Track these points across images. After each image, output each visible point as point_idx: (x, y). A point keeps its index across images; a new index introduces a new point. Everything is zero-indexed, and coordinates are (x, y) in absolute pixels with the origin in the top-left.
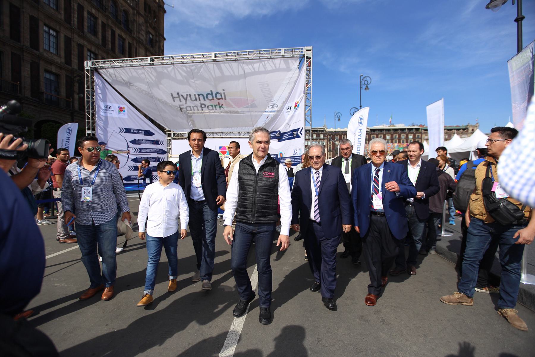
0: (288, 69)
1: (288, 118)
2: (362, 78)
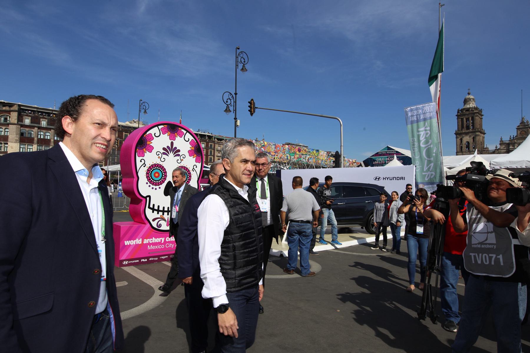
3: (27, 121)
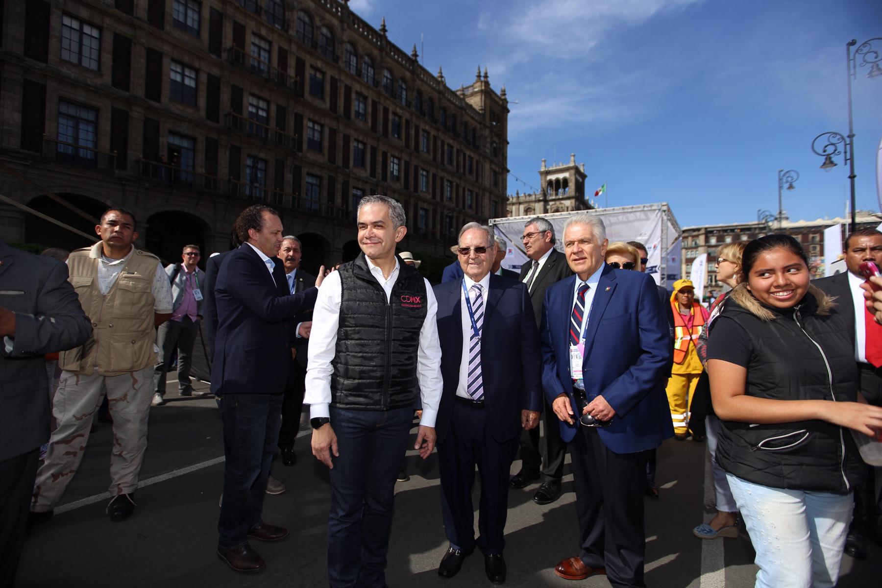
0: (648, 219)
2: (782, 173)
3: (713, 241)
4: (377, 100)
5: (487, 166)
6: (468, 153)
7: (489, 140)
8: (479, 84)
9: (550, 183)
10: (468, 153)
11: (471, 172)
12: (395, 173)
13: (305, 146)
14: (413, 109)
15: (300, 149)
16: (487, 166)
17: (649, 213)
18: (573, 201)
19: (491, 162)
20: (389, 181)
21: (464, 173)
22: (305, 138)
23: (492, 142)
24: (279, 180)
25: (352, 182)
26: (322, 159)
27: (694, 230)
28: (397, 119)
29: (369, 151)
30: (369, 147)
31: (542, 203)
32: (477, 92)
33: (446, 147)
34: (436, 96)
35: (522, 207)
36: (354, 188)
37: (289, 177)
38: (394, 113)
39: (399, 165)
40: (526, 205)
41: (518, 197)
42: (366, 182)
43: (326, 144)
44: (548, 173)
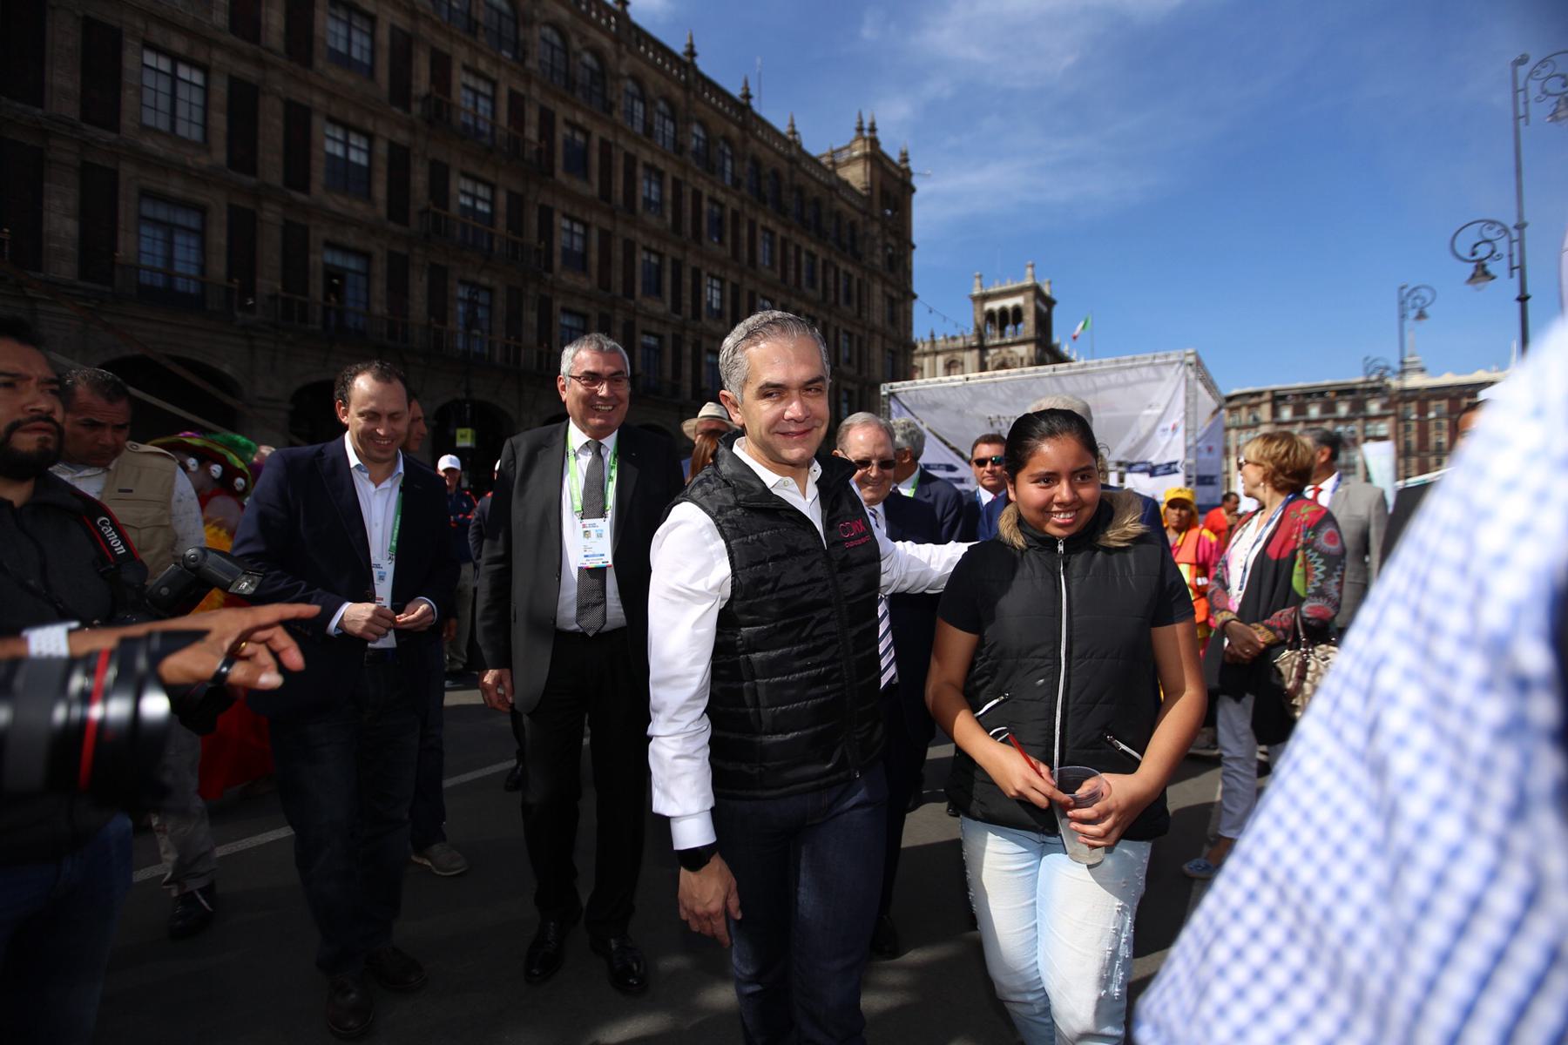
0: (1161, 379)
1: (1163, 442)
2: (1406, 291)
3: (1286, 414)
4: (680, 177)
5: (877, 288)
6: (842, 266)
7: (879, 242)
8: (860, 143)
9: (990, 316)
10: (842, 266)
11: (848, 300)
12: (715, 305)
13: (557, 261)
14: (744, 191)
15: (549, 269)
16: (877, 288)
17: (1163, 369)
18: (1032, 347)
19: (885, 281)
20: (704, 319)
21: (837, 302)
22: (557, 248)
23: (885, 246)
24: (514, 322)
25: (640, 323)
26: (588, 284)
27: (1252, 395)
28: (716, 209)
29: (668, 267)
30: (668, 260)
31: (976, 352)
32: (857, 158)
33: (804, 257)
34: (784, 166)
35: (941, 360)
36: (645, 332)
37: (531, 317)
38: (712, 200)
39: (721, 290)
40: (947, 356)
41: (933, 342)
42: (665, 323)
43: (594, 257)
44: (986, 297)
